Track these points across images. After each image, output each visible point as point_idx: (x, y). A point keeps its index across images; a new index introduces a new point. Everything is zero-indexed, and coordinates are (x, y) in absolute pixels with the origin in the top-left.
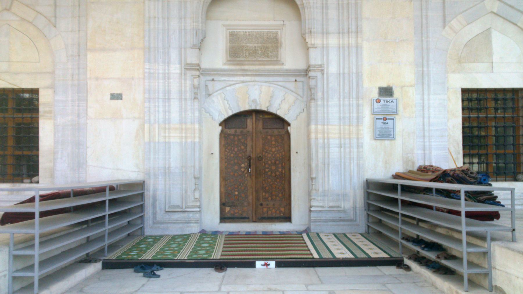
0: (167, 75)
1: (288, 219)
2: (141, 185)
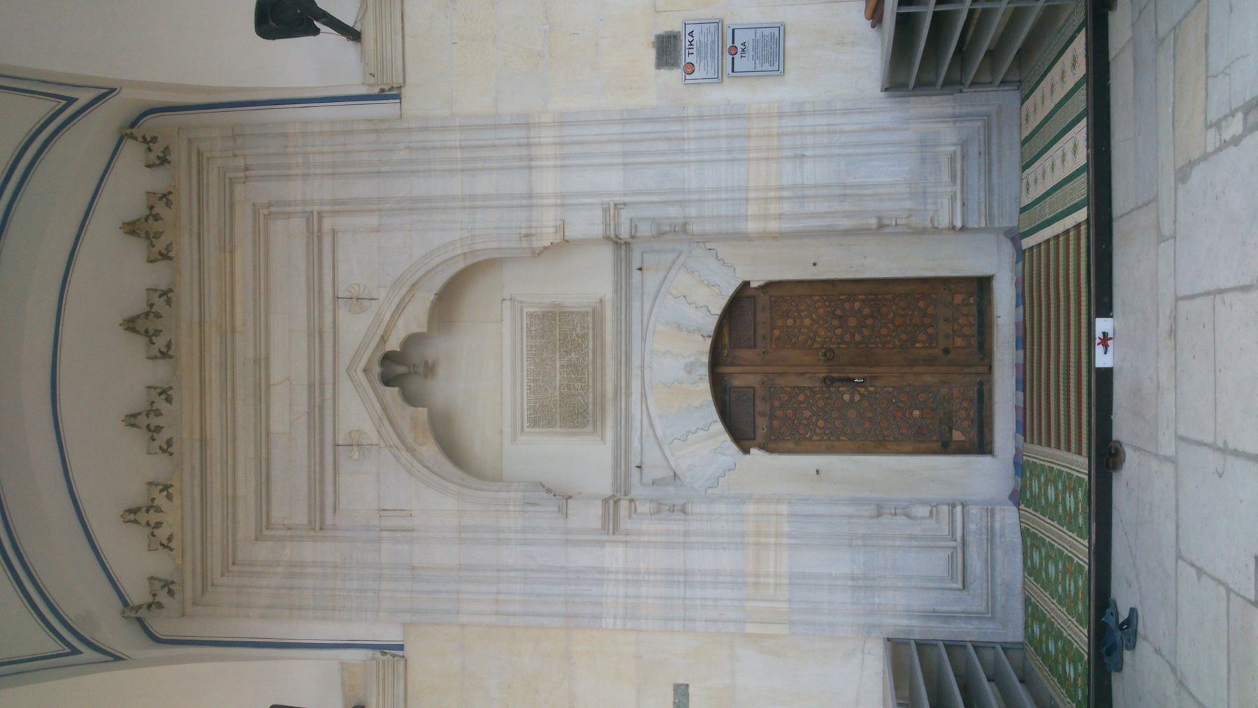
0: (629, 577)
1: (983, 285)
2: (896, 647)
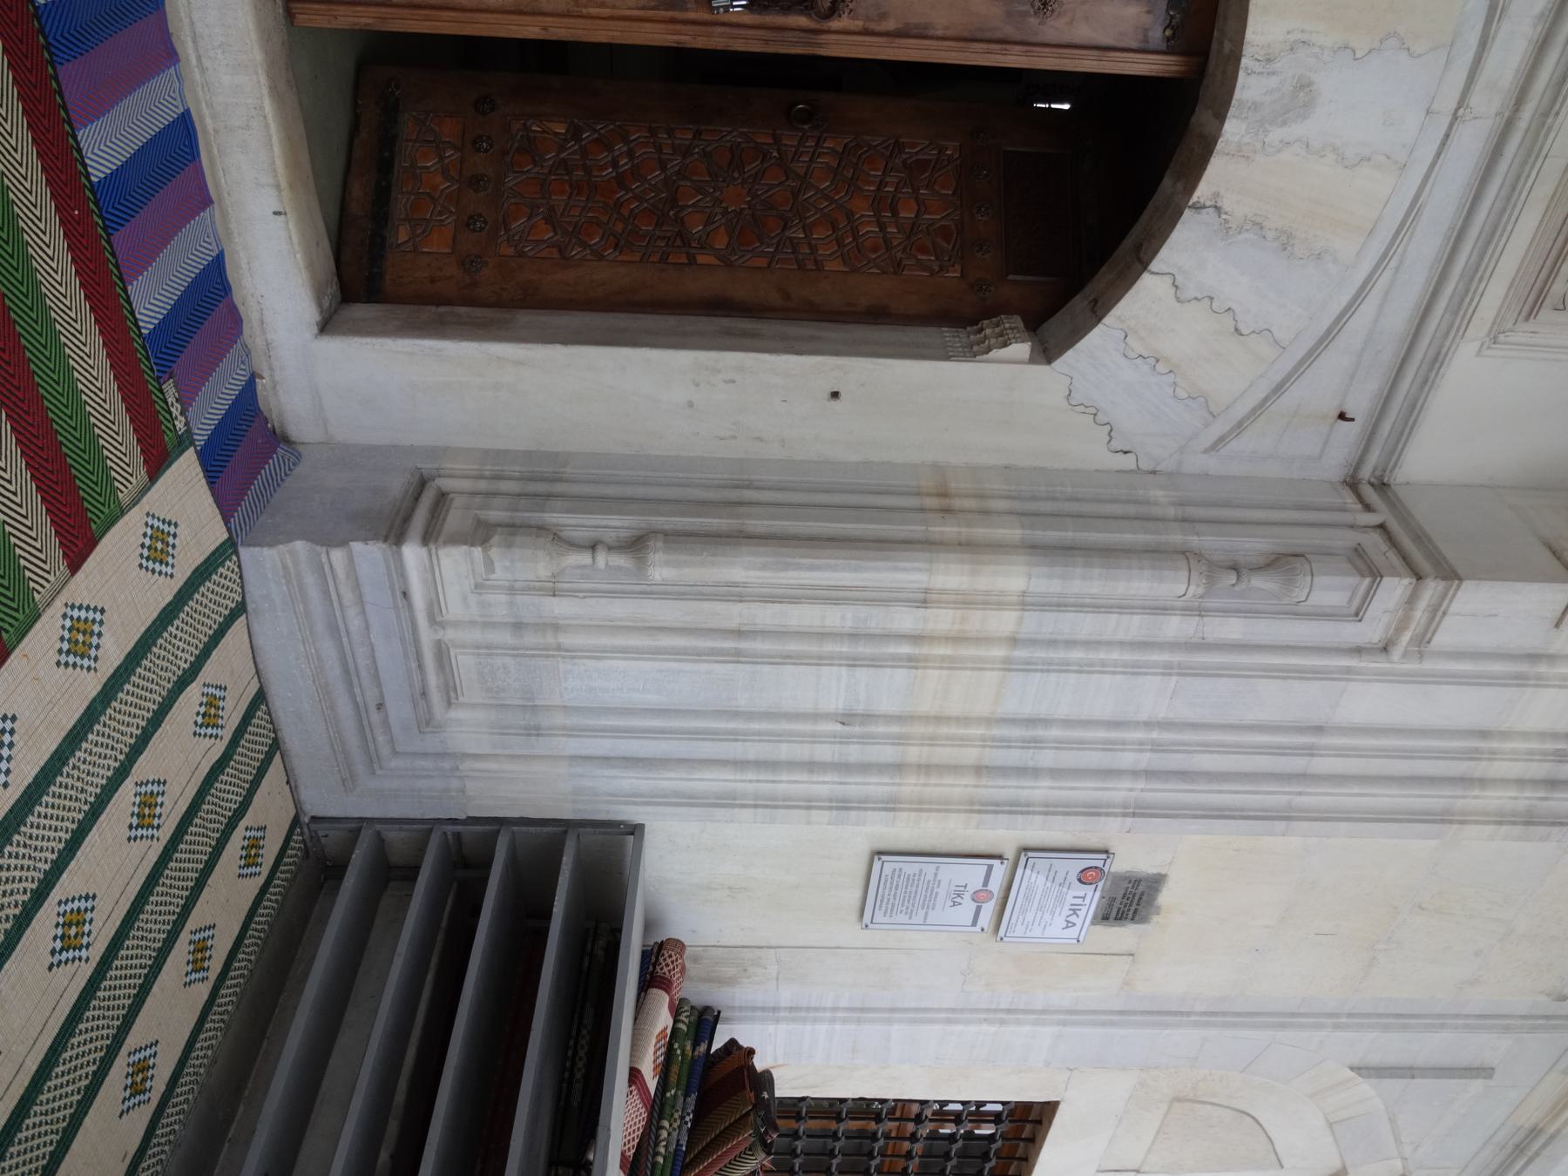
1: (365, 278)
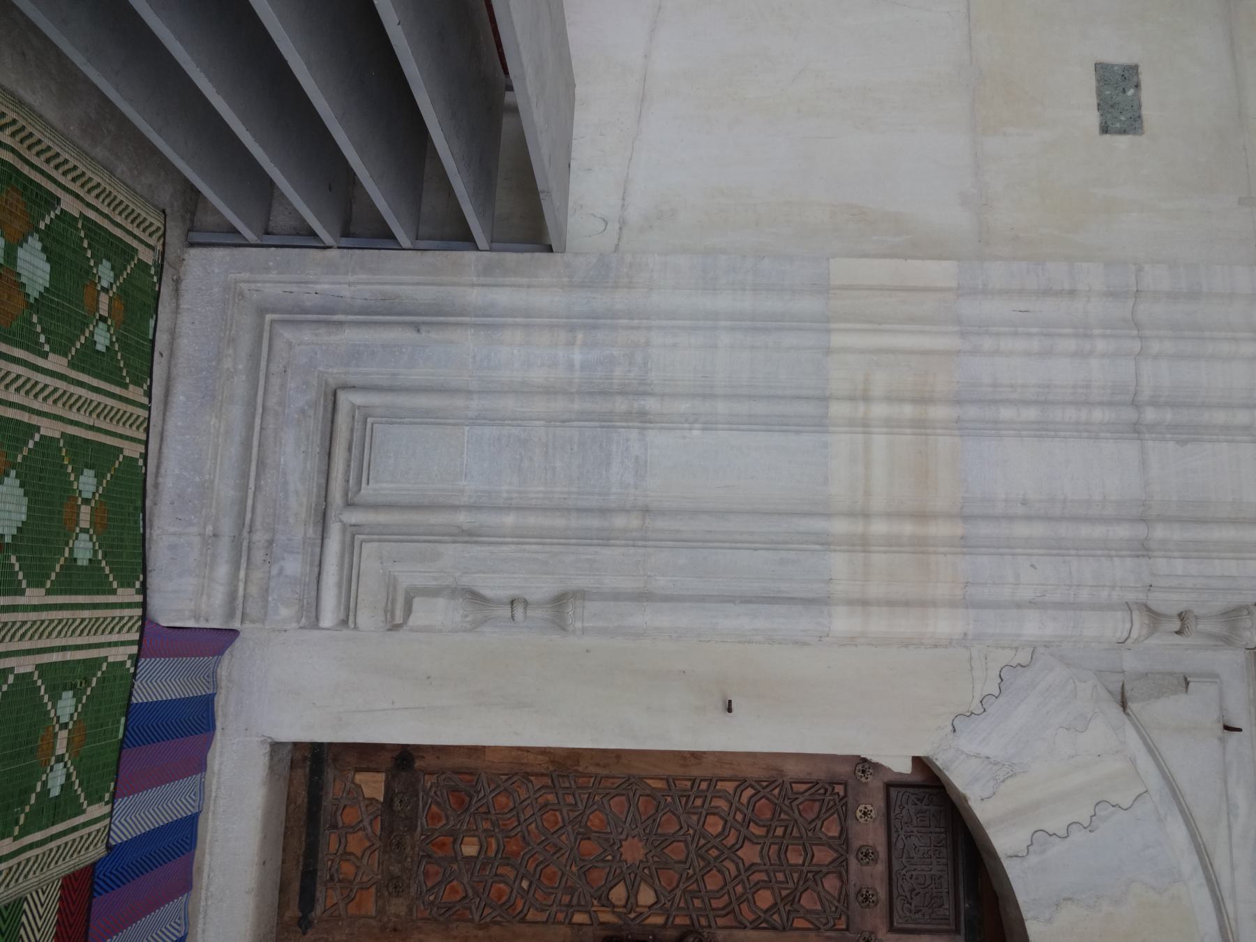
2: (528, 225)
